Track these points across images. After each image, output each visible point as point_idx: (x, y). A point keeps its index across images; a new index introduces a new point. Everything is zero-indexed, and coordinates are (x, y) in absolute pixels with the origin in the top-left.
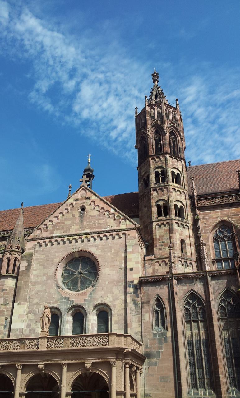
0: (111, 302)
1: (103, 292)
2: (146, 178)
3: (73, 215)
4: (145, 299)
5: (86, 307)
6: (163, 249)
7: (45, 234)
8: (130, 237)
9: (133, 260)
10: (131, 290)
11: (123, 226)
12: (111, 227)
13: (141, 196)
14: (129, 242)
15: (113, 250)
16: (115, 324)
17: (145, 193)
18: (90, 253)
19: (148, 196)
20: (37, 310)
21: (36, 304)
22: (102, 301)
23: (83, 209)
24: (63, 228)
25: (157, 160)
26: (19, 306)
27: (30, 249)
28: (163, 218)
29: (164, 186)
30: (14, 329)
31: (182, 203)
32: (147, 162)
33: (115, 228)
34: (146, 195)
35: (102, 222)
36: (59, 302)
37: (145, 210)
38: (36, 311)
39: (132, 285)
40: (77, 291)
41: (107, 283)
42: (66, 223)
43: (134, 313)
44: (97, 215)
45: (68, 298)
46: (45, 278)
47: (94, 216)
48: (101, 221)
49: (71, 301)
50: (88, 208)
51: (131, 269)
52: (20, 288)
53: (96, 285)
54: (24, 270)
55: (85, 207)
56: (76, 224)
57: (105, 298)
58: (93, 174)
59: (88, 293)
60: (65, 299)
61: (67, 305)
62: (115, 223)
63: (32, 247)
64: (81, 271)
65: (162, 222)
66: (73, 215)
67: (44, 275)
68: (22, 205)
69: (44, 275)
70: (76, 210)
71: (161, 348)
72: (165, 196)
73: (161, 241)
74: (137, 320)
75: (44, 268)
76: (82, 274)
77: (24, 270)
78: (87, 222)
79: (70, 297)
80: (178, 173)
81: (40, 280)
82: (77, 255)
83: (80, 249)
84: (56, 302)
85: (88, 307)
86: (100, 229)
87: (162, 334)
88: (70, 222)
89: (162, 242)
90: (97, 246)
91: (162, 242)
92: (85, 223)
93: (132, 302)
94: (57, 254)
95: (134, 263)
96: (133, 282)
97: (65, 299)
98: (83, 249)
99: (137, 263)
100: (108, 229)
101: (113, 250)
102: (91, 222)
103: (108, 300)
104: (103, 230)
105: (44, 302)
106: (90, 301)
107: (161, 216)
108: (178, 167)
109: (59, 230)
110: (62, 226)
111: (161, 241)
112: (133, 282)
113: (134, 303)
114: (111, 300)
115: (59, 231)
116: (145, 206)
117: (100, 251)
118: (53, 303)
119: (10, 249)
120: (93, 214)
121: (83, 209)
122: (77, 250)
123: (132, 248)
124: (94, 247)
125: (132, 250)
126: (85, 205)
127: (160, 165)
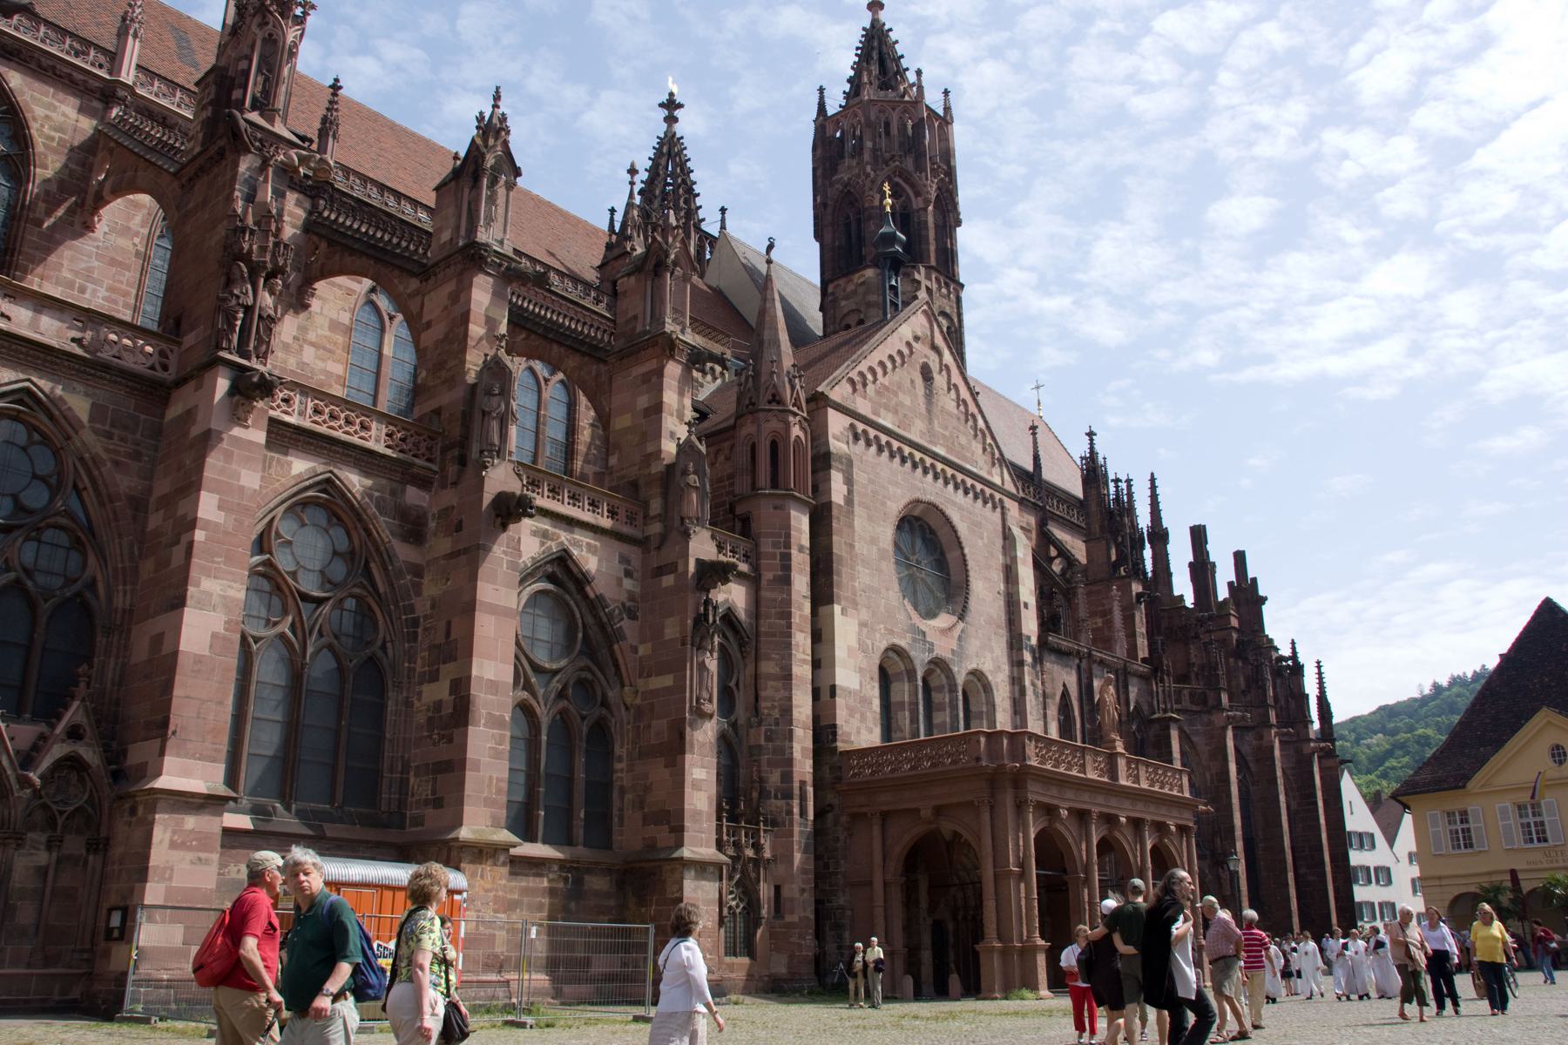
3: (912, 382)
5: (955, 669)
10: (1028, 657)
11: (997, 480)
25: (944, 291)
30: (844, 689)
33: (984, 474)
47: (950, 414)
48: (963, 440)
52: (840, 557)
75: (870, 518)
83: (932, 499)
90: (961, 508)
94: (891, 488)
103: (987, 667)
104: (968, 467)
112: (1029, 638)
124: (961, 510)
127: (948, 310)
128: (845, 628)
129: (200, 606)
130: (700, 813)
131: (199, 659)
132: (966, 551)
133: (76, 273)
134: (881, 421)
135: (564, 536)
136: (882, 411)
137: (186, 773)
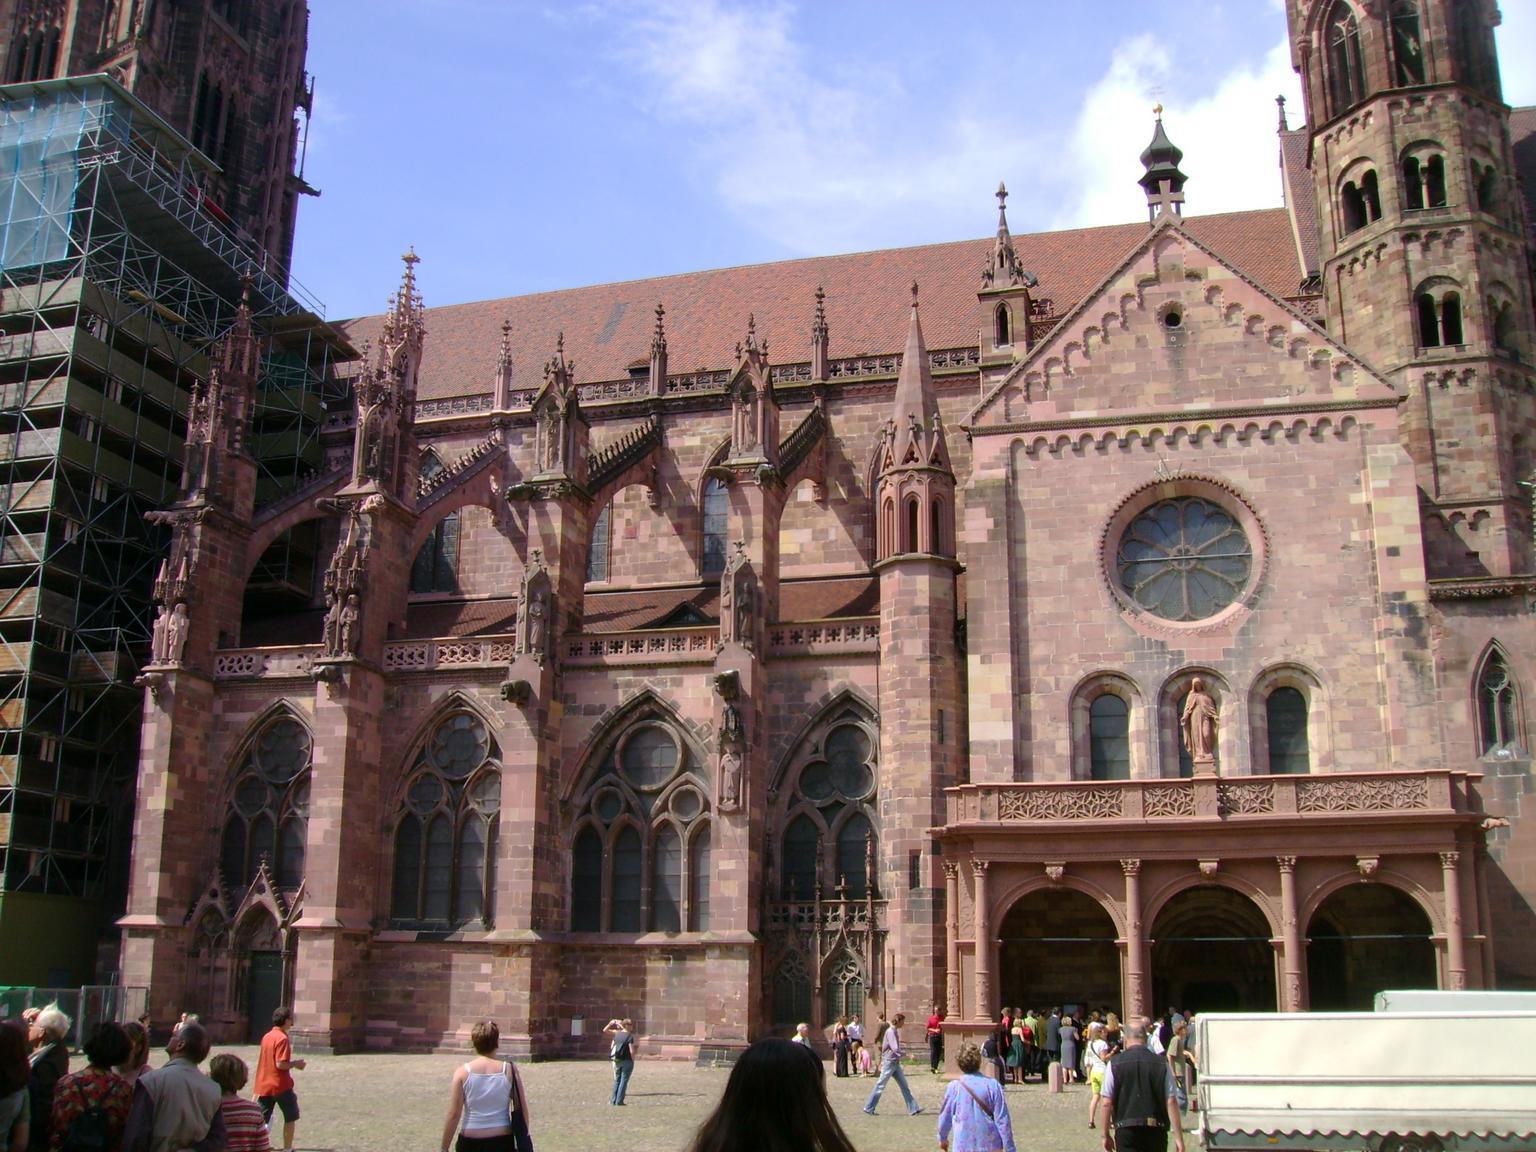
0: (1320, 659)
1: (1288, 627)
2: (1358, 184)
4: (1452, 658)
6: (1452, 472)
7: (1038, 412)
8: (1376, 433)
9: (1396, 519)
11: (1342, 393)
12: (1295, 391)
13: (1342, 256)
14: (1375, 451)
15: (1312, 478)
16: (1341, 731)
17: (1364, 244)
18: (1222, 487)
19: (1378, 258)
20: (1051, 680)
21: (1044, 660)
22: (1286, 656)
23: (1172, 318)
24: (1104, 391)
26: (987, 666)
27: (991, 468)
28: (1451, 352)
29: (1448, 224)
31: (1509, 291)
32: (1369, 114)
33: (1310, 397)
34: (1368, 254)
35: (1260, 373)
36: (1130, 656)
37: (1363, 312)
38: (1047, 684)
39: (1401, 605)
40: (1182, 620)
41: (1300, 595)
42: (1116, 368)
43: (1411, 698)
44: (1237, 344)
45: (1163, 644)
46: (1062, 573)
47: (1226, 347)
48: (1255, 370)
49: (1172, 653)
50: (1194, 313)
51: (1393, 552)
53: (1262, 602)
54: (984, 539)
55: (1180, 307)
56: (1158, 376)
57: (1298, 649)
58: (1182, 167)
59: (1235, 630)
60: (1150, 648)
61: (1161, 666)
62: (1313, 379)
63: (997, 458)
64: (1187, 551)
65: (1448, 368)
66: (1138, 340)
67: (1059, 560)
68: (915, 290)
69: (1059, 560)
70: (1149, 322)
71: (1512, 809)
72: (1454, 266)
73: (1444, 441)
74: (1423, 720)
76: (1193, 563)
77: (984, 539)
78: (1200, 371)
79: (1168, 639)
80: (1488, 169)
81: (1044, 578)
82: (1170, 492)
83: (1184, 471)
84: (1118, 656)
85: (1240, 675)
86: (1254, 396)
87: (1515, 767)
88: (1130, 368)
89: (1451, 445)
90: (1250, 462)
91: (1451, 445)
92: (1192, 374)
93: (1405, 664)
94: (1095, 488)
95: (1401, 530)
96: (1400, 595)
97: (1150, 648)
98: (1194, 473)
99: (1409, 529)
100: (1285, 401)
101: (1312, 478)
102: (1217, 368)
104: (1269, 402)
105: (1075, 656)
106: (1242, 655)
107: (1435, 343)
108: (1489, 143)
109: (1092, 396)
110: (1101, 382)
111: (1444, 441)
112: (1400, 595)
113: (1412, 667)
114: (1321, 652)
115: (1093, 401)
116: (1364, 298)
117: (1263, 480)
118: (1107, 658)
119: (912, 465)
120: (1220, 341)
121: (1172, 318)
122: (1175, 473)
123: (1389, 475)
124: (1237, 466)
125: (1391, 481)
126: (1183, 300)
128: (988, 678)
129: (319, 815)
130: (729, 899)
131: (317, 847)
132: (1262, 513)
133: (492, 559)
134: (1075, 415)
135: (647, 681)
136: (1077, 402)
137: (314, 915)
